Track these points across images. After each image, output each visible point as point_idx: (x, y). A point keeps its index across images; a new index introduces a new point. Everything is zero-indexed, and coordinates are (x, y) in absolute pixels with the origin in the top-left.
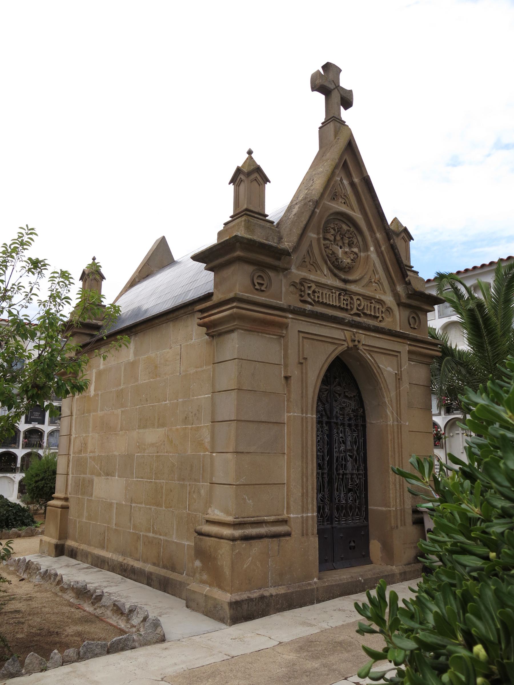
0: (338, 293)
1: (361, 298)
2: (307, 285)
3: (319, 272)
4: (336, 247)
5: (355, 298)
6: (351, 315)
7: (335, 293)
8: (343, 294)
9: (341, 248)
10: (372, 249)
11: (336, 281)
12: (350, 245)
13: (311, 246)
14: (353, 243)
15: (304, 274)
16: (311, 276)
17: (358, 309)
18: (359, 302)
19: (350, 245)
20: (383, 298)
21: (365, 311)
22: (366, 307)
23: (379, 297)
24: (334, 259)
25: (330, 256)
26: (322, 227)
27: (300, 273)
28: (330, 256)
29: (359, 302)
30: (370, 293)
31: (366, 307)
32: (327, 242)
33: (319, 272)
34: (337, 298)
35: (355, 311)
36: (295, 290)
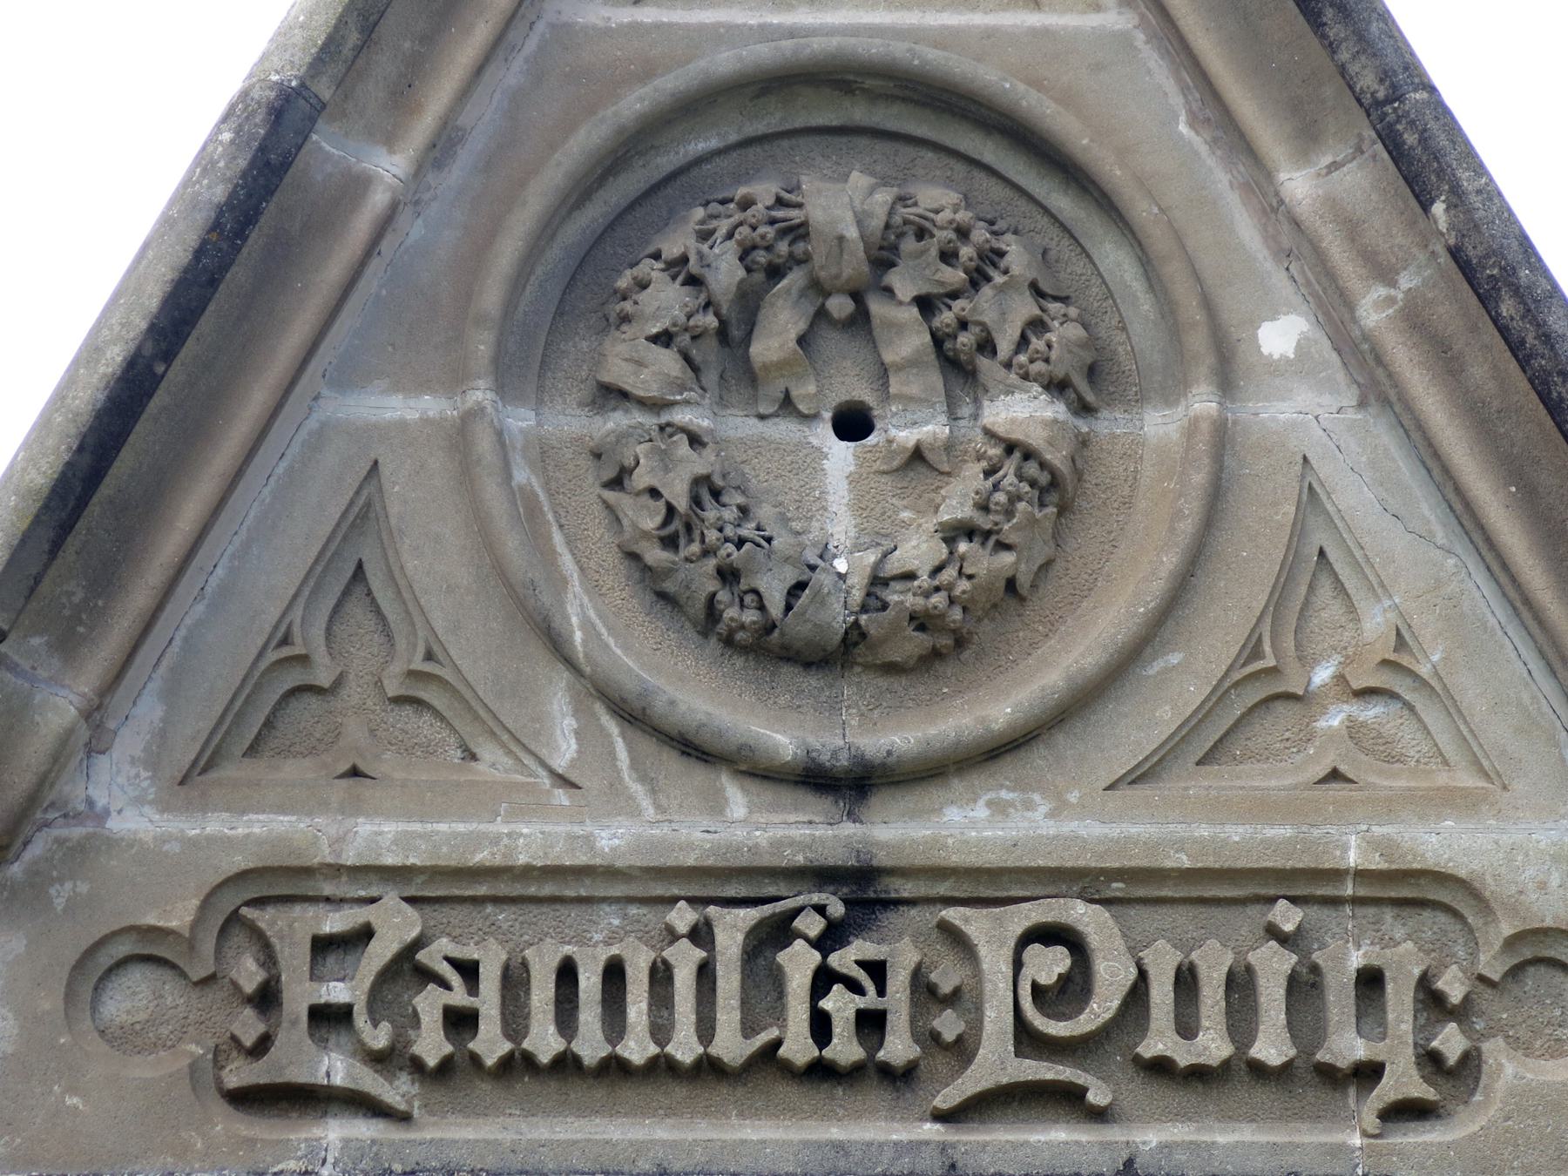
0: (732, 928)
1: (1080, 914)
2: (294, 928)
3: (489, 753)
4: (784, 430)
5: (992, 933)
6: (941, 1117)
7: (701, 935)
8: (812, 925)
9: (853, 424)
10: (1281, 335)
11: (716, 806)
12: (959, 367)
13: (363, 515)
14: (987, 346)
15: (254, 826)
16: (365, 828)
17: (1027, 1039)
18: (1049, 964)
19: (959, 367)
20: (1438, 842)
21: (1159, 1041)
22: (1162, 994)
23: (1374, 844)
24: (702, 579)
25: (655, 555)
26: (491, 297)
27: (215, 825)
28: (655, 555)
29: (1049, 964)
30: (1236, 833)
31: (1162, 994)
32: (619, 420)
33: (489, 753)
34: (729, 982)
35: (997, 1062)
36: (174, 995)
